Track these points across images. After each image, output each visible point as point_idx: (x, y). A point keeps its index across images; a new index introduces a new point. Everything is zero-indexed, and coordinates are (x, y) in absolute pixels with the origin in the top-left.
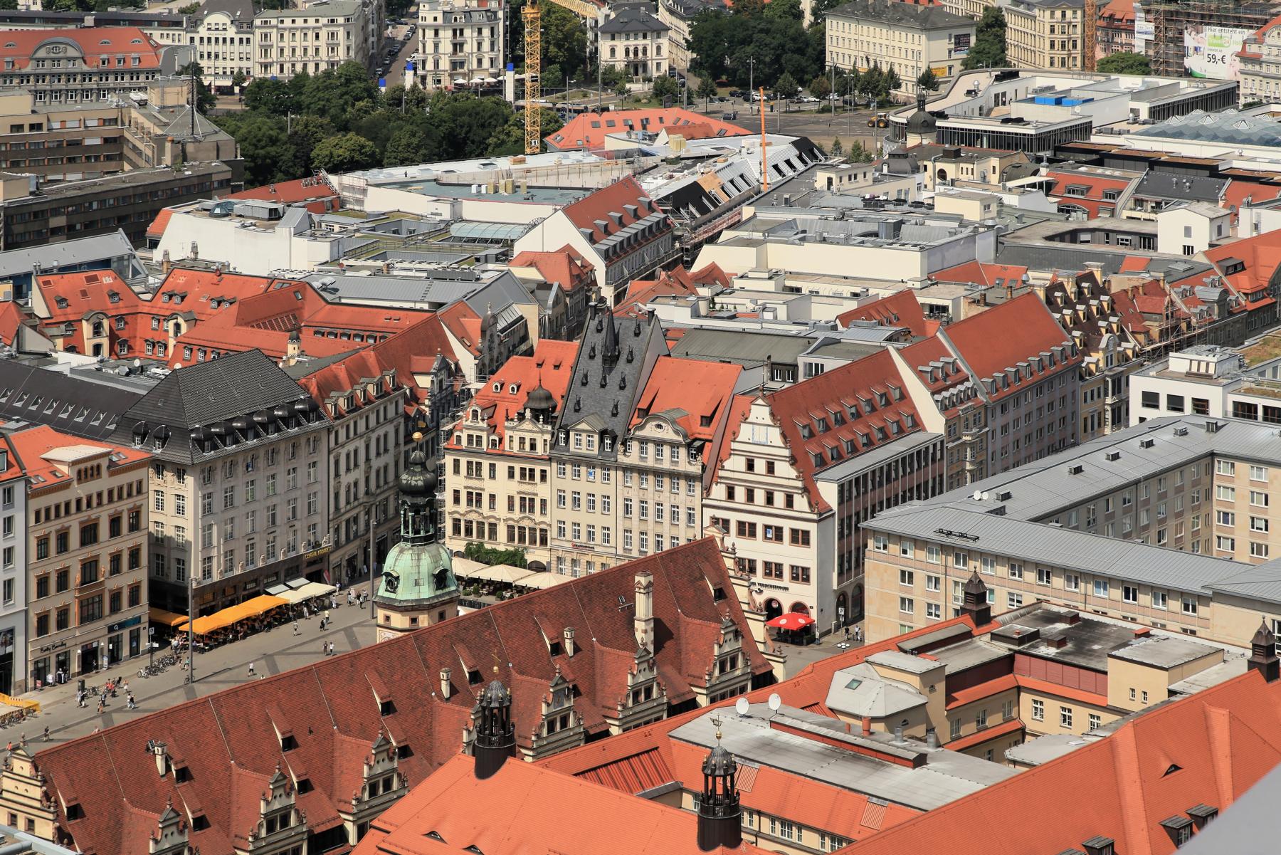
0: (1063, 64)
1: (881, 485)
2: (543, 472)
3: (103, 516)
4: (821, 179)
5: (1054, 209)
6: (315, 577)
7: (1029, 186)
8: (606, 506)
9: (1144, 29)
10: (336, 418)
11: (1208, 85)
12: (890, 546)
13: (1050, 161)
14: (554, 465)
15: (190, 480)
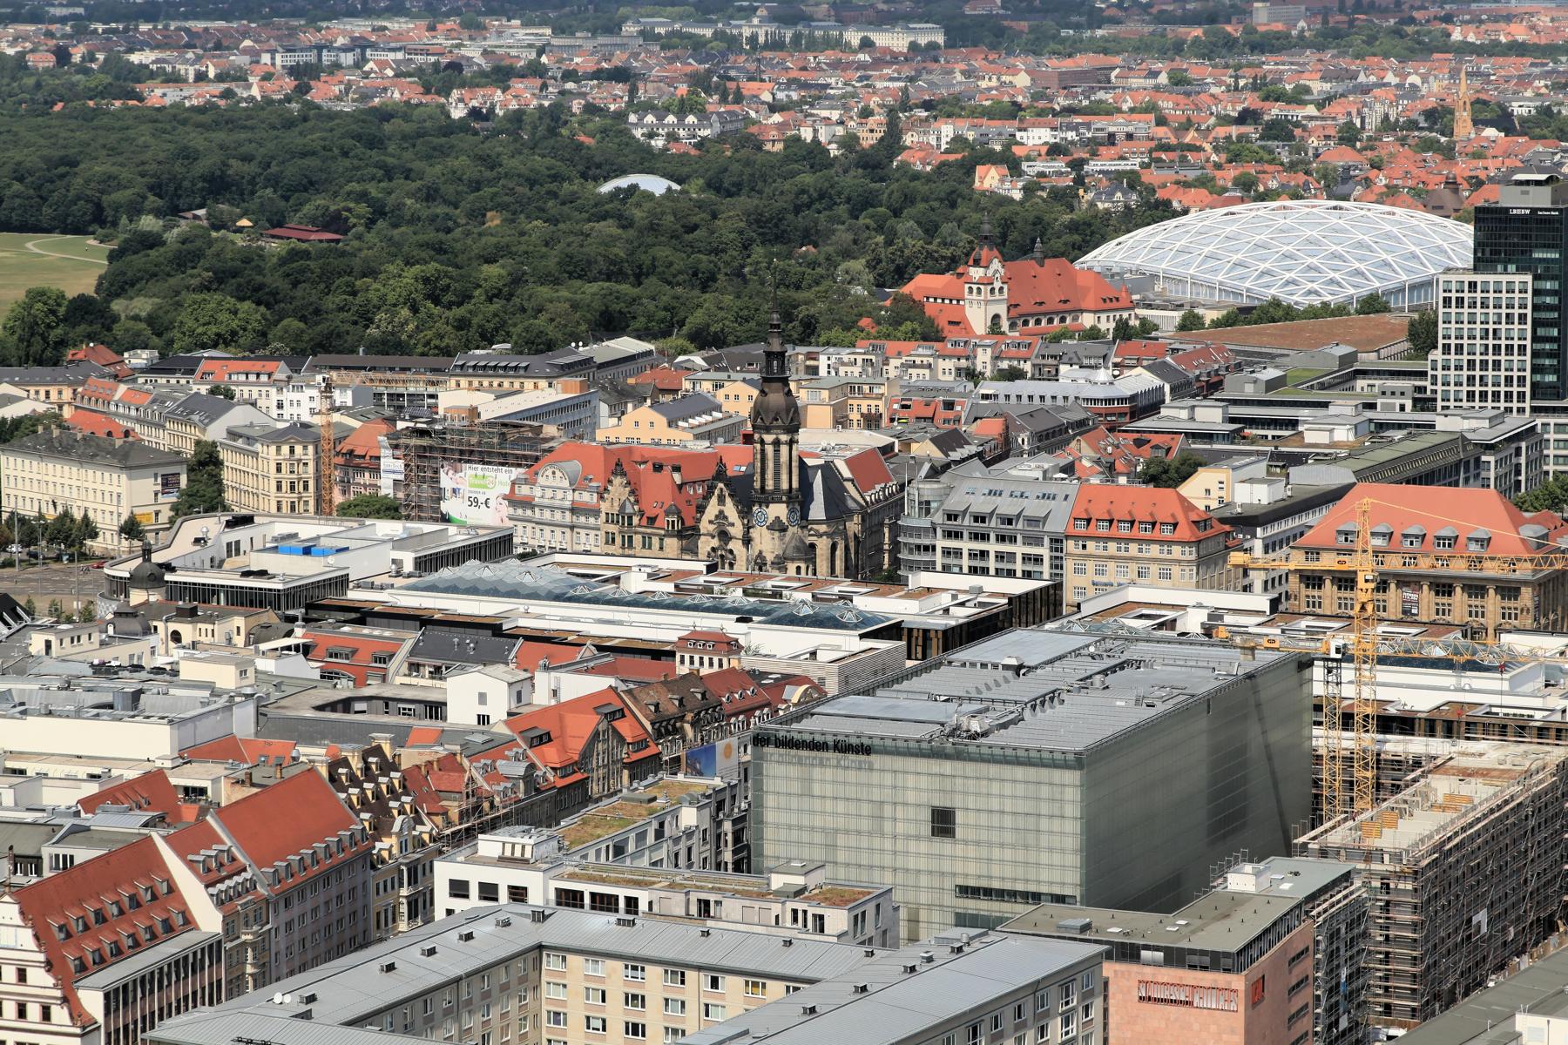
0: (293, 509)
4: (37, 642)
5: (316, 675)
9: (392, 467)
11: (481, 532)
13: (307, 620)
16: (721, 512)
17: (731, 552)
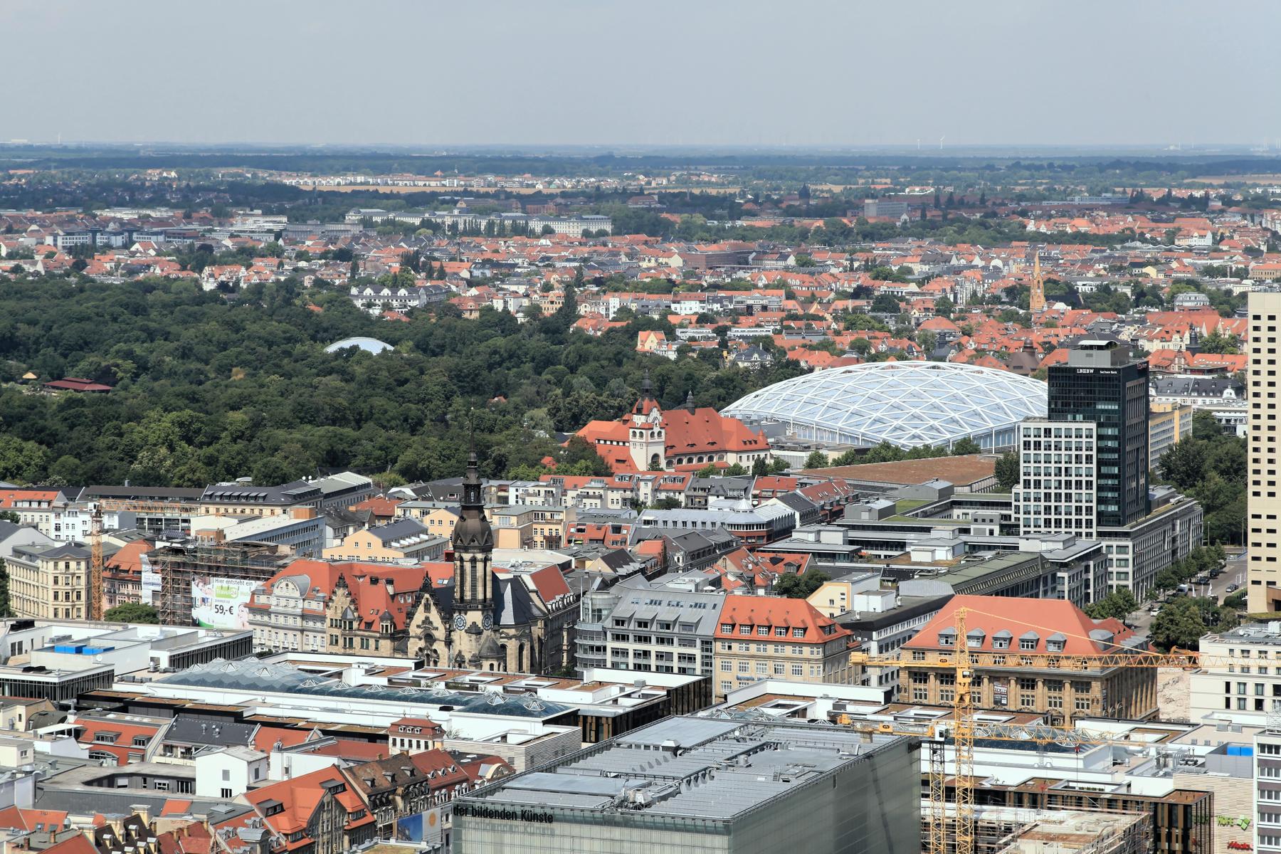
0: (67, 615)
5: (86, 755)
7: (58, 733)
9: (151, 580)
11: (226, 634)
13: (78, 709)
16: (427, 618)
17: (435, 651)
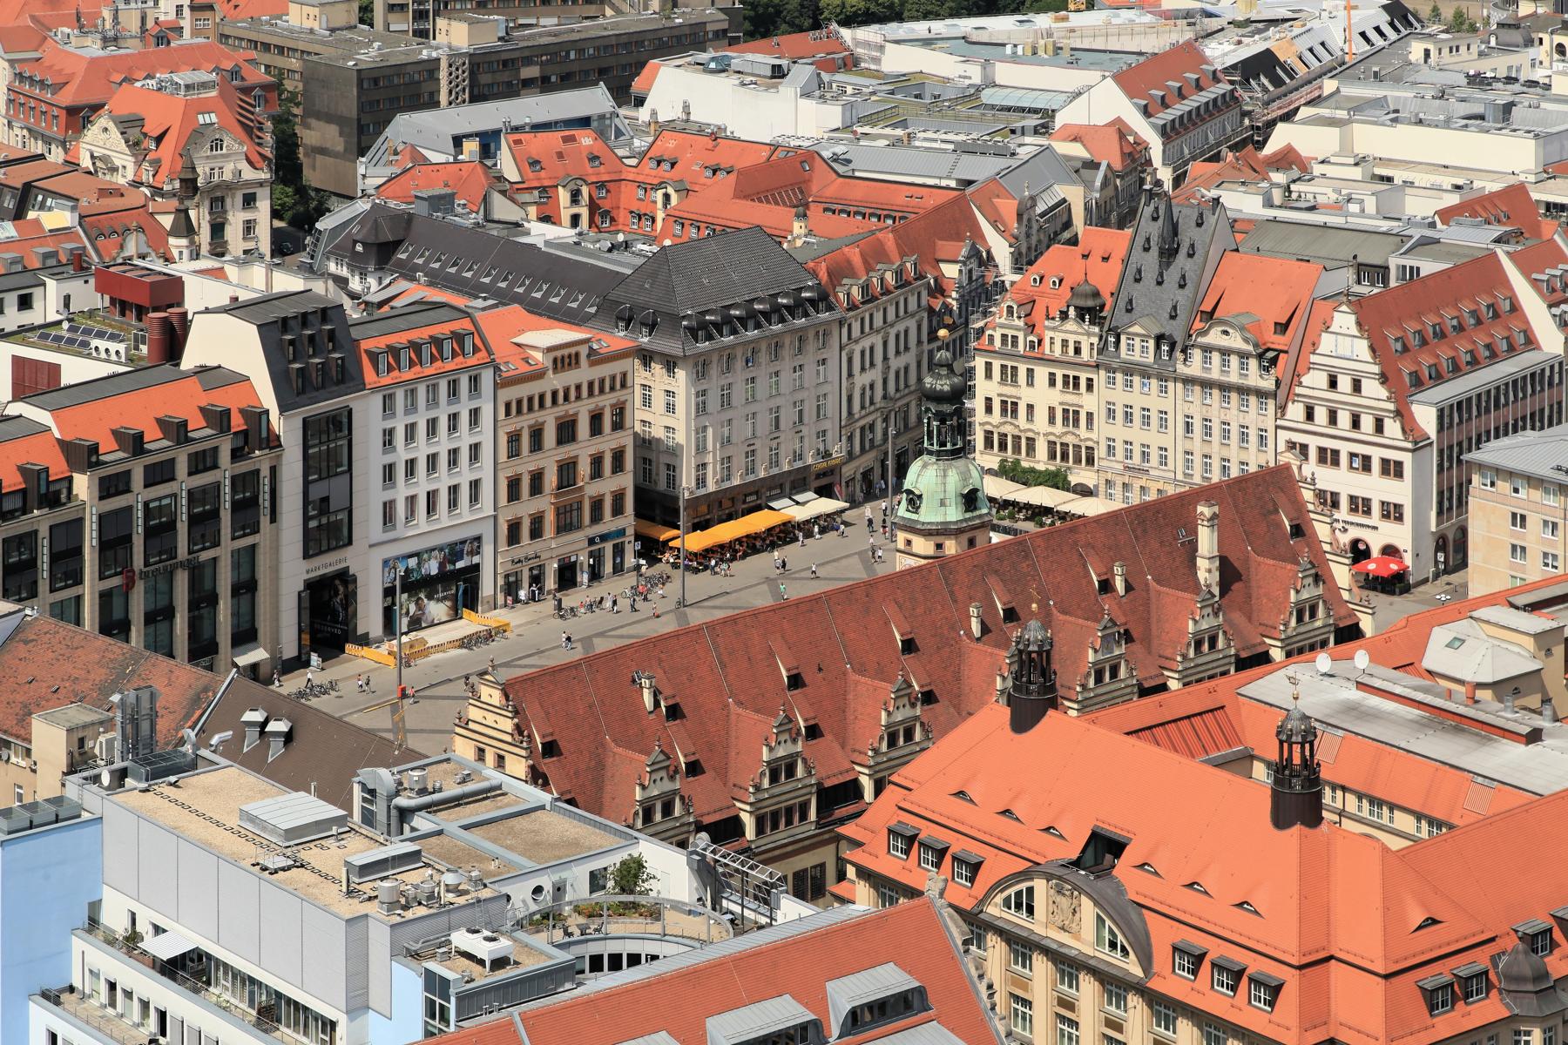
1: (1488, 411)
2: (1090, 380)
3: (582, 411)
4: (1416, 50)
6: (825, 492)
8: (1163, 423)
10: (849, 310)
12: (1499, 483)
14: (1102, 372)
15: (681, 374)
